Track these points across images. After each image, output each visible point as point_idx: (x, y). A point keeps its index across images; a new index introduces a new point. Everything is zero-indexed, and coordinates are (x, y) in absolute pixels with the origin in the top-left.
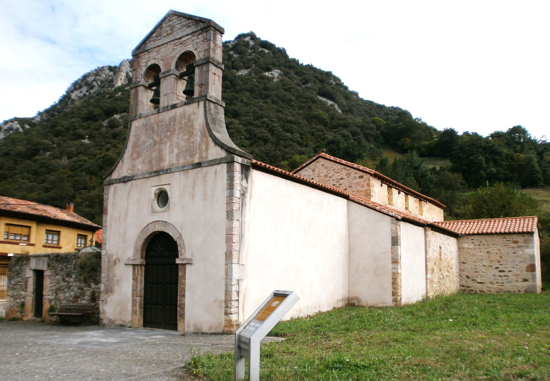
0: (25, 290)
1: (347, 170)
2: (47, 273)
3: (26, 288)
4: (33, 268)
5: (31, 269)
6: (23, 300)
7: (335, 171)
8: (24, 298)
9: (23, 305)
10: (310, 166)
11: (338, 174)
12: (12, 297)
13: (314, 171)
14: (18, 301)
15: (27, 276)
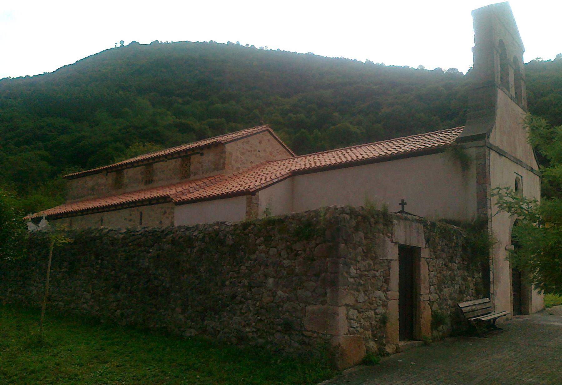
0: (386, 286)
1: (288, 155)
2: (425, 253)
3: (387, 281)
4: (402, 242)
5: (396, 243)
6: (381, 310)
7: (278, 151)
8: (385, 305)
9: (384, 320)
10: (258, 135)
11: (280, 155)
12: (353, 307)
13: (260, 142)
14: (371, 313)
15: (390, 258)
